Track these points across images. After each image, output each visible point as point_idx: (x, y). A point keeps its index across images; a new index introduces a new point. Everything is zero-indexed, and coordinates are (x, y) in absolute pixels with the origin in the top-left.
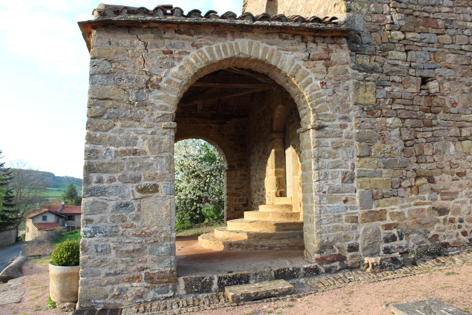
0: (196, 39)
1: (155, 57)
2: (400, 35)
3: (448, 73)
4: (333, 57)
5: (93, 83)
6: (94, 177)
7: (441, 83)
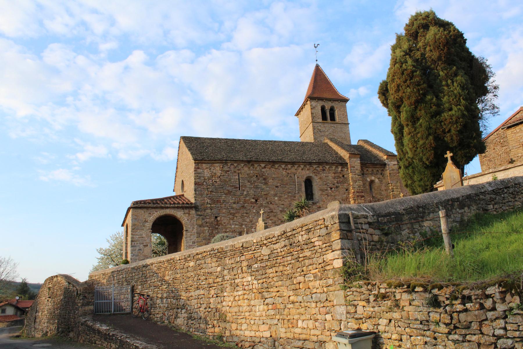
0: (156, 210)
1: (147, 215)
2: (209, 206)
4: (191, 213)
6: (133, 243)
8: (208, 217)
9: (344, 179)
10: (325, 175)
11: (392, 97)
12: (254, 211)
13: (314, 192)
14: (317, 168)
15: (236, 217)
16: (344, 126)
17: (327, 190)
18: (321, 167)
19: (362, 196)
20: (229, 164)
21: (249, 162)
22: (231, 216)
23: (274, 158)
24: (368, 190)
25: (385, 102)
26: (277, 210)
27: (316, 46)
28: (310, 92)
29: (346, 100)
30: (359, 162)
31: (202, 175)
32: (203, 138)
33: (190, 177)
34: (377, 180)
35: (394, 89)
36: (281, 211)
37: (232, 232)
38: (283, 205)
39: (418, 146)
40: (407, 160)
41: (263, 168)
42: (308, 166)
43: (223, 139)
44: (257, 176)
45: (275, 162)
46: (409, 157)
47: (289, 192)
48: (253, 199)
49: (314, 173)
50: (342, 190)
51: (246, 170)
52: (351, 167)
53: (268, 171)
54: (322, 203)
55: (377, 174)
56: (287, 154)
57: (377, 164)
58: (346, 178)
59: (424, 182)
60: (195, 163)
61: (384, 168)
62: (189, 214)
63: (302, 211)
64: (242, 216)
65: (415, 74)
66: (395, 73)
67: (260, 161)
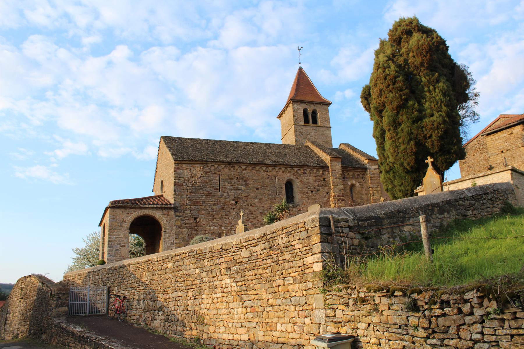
0: (135, 210)
1: (125, 215)
2: (189, 207)
3: (203, 216)
4: (170, 213)
5: (110, 221)
6: (110, 243)
7: (200, 219)
8: (187, 218)
9: (324, 182)
10: (306, 178)
11: (375, 101)
12: (234, 213)
13: (294, 195)
14: (298, 171)
15: (216, 218)
16: (326, 129)
17: (307, 193)
18: (302, 170)
19: (343, 200)
20: (210, 165)
21: (229, 163)
22: (210, 218)
23: (255, 161)
24: (349, 194)
25: (367, 106)
26: (258, 213)
27: (300, 48)
28: (293, 94)
29: (328, 104)
30: (340, 165)
31: (182, 176)
32: (184, 138)
33: (170, 178)
34: (358, 184)
35: (377, 94)
36: (261, 214)
37: (211, 233)
38: (263, 207)
39: (399, 151)
40: (388, 164)
41: (243, 170)
42: (289, 169)
43: (204, 140)
44: (237, 178)
45: (256, 164)
46: (390, 162)
47: (270, 195)
48: (233, 200)
49: (295, 175)
50: (322, 193)
51: (227, 172)
52: (332, 171)
53: (249, 173)
54: (303, 206)
55: (358, 178)
56: (268, 156)
57: (358, 168)
58: (327, 181)
59: (404, 187)
60: (175, 163)
61: (365, 172)
62: (168, 215)
63: (282, 213)
64: (222, 218)
65: (397, 79)
66: (378, 78)
67: (241, 163)
